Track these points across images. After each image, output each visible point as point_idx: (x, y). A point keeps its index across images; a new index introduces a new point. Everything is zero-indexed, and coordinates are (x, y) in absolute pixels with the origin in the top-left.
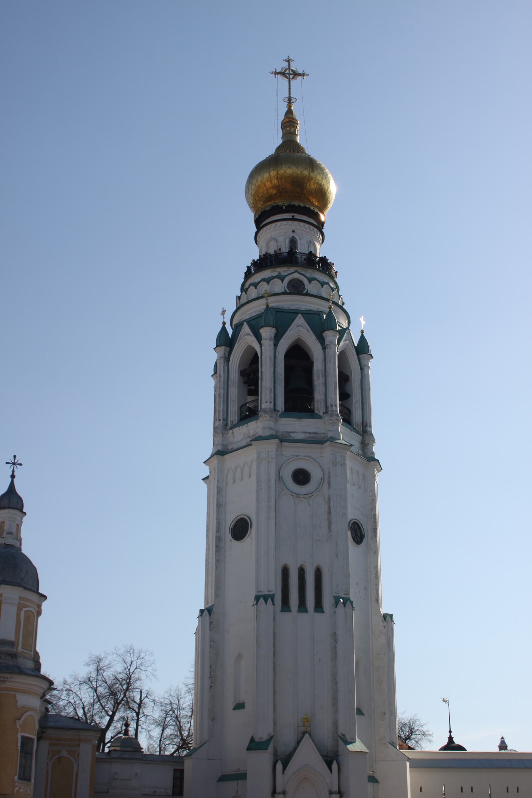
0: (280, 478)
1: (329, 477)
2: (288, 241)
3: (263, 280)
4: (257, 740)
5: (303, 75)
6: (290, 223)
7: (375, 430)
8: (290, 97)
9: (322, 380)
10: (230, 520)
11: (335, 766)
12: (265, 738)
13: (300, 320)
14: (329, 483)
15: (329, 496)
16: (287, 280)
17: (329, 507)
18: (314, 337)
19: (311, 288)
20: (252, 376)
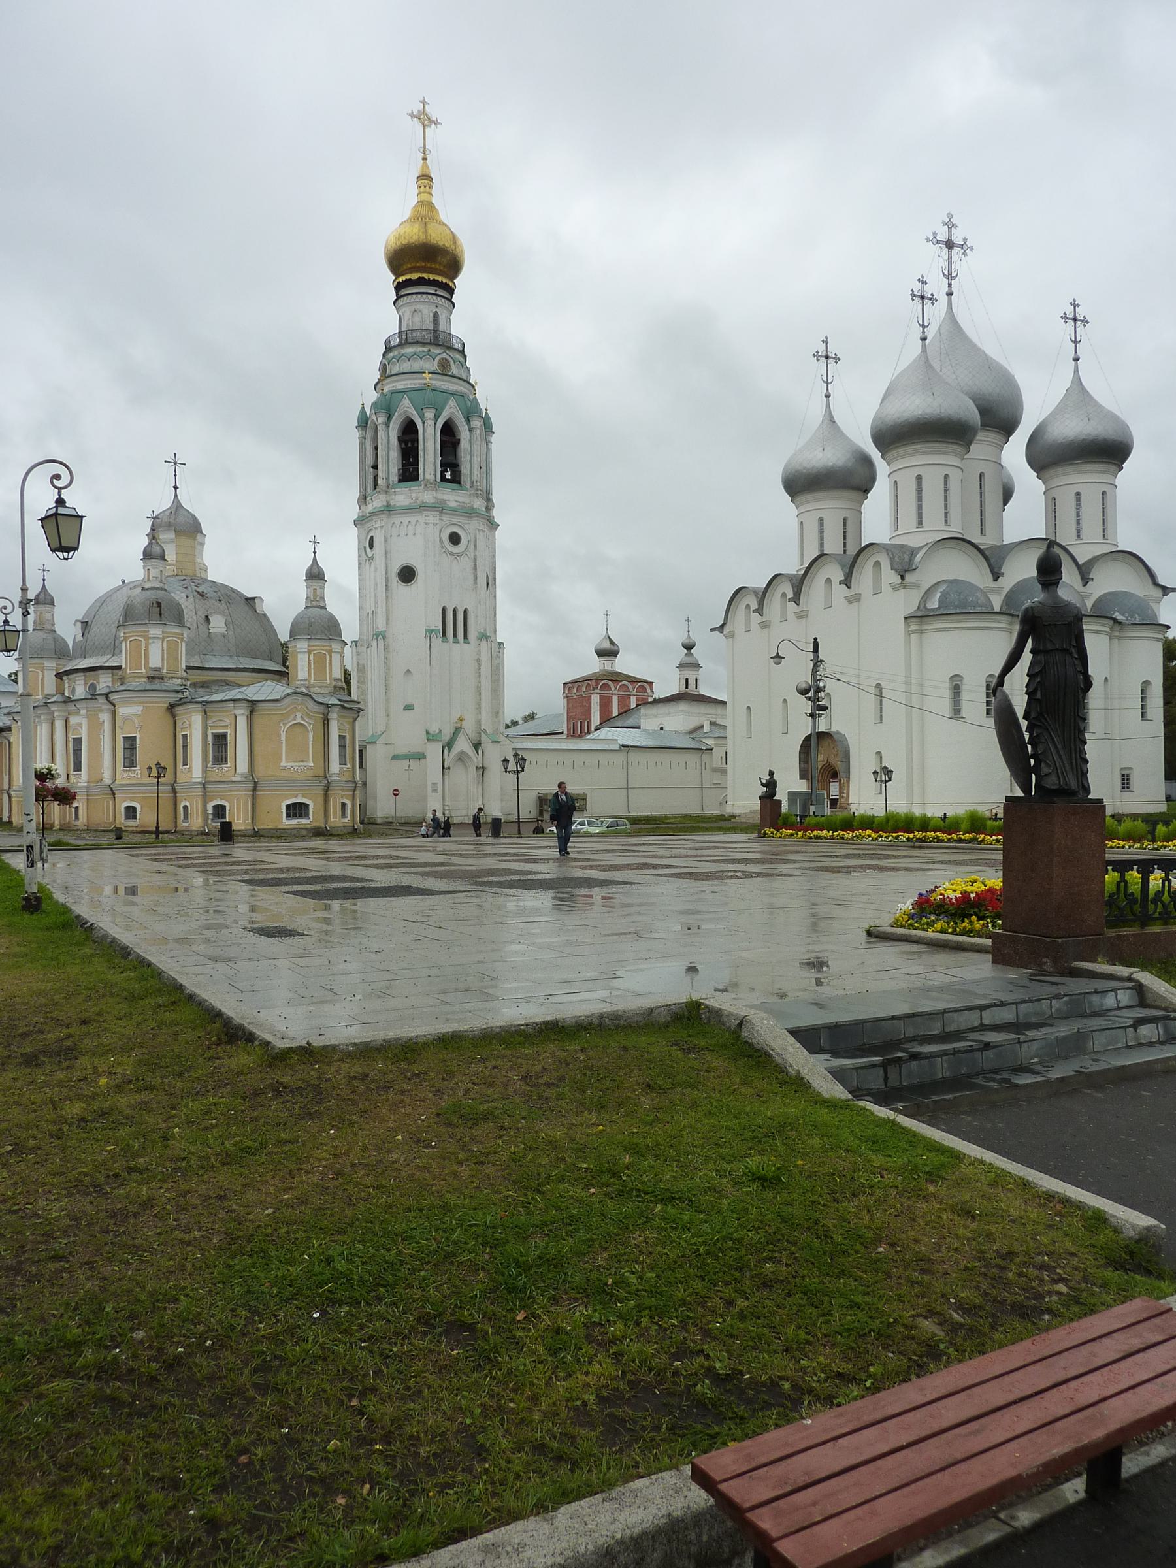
0: (441, 539)
1: (475, 541)
2: (431, 315)
3: (415, 354)
4: (431, 732)
5: (436, 123)
6: (435, 297)
7: (494, 497)
8: (425, 148)
9: (468, 458)
10: (396, 567)
11: (480, 752)
12: (437, 731)
13: (452, 403)
14: (475, 546)
15: (475, 556)
16: (437, 360)
17: (475, 565)
18: (463, 419)
19: (455, 369)
20: (410, 445)
